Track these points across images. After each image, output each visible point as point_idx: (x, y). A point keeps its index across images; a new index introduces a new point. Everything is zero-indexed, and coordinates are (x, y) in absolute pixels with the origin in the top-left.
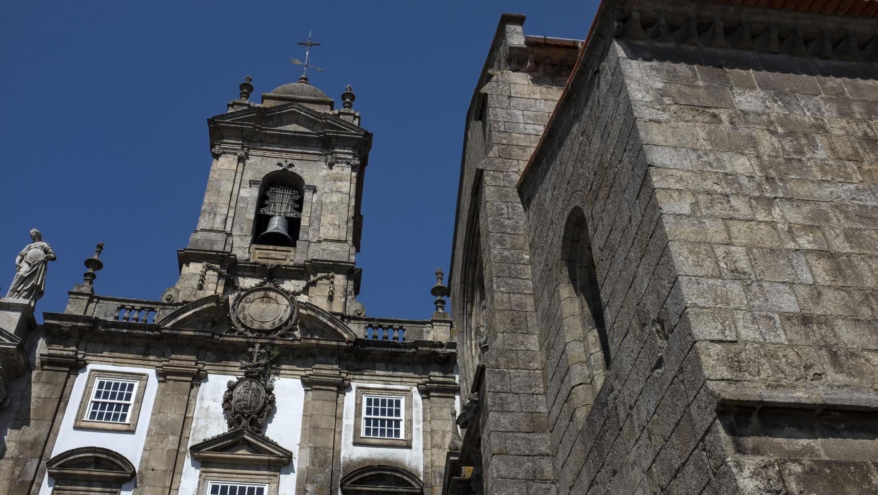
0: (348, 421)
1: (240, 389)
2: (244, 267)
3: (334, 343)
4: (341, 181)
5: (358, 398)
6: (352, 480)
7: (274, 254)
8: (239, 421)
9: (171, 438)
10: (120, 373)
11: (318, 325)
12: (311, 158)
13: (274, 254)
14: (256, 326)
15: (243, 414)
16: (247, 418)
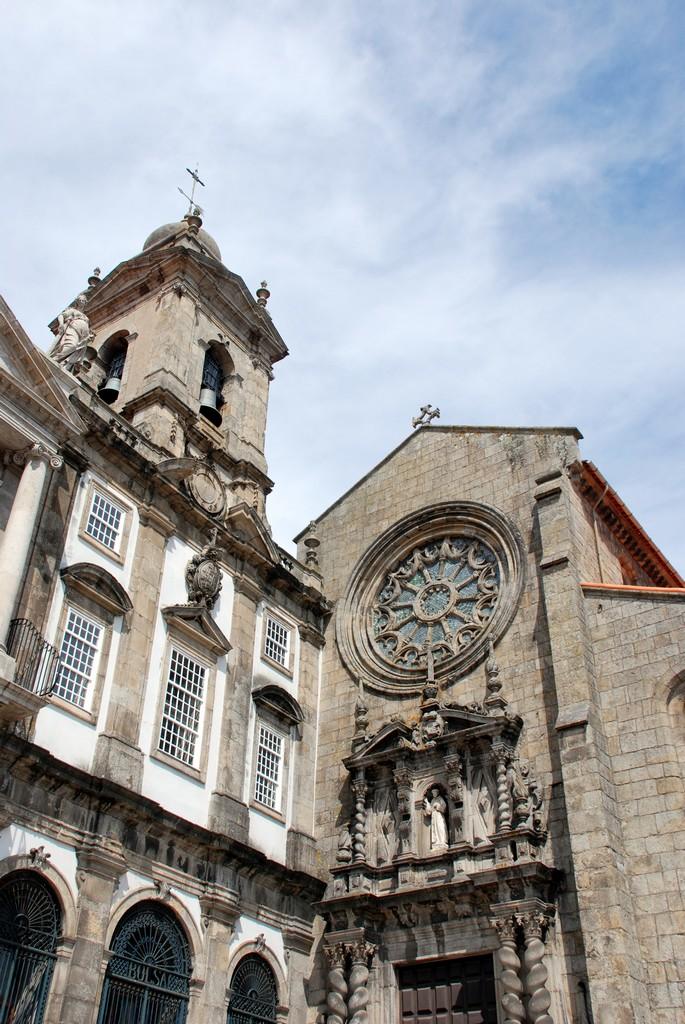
1: (205, 568)
2: (194, 433)
8: (198, 598)
10: (114, 496)
11: (251, 532)
12: (241, 346)
13: (213, 433)
16: (207, 598)
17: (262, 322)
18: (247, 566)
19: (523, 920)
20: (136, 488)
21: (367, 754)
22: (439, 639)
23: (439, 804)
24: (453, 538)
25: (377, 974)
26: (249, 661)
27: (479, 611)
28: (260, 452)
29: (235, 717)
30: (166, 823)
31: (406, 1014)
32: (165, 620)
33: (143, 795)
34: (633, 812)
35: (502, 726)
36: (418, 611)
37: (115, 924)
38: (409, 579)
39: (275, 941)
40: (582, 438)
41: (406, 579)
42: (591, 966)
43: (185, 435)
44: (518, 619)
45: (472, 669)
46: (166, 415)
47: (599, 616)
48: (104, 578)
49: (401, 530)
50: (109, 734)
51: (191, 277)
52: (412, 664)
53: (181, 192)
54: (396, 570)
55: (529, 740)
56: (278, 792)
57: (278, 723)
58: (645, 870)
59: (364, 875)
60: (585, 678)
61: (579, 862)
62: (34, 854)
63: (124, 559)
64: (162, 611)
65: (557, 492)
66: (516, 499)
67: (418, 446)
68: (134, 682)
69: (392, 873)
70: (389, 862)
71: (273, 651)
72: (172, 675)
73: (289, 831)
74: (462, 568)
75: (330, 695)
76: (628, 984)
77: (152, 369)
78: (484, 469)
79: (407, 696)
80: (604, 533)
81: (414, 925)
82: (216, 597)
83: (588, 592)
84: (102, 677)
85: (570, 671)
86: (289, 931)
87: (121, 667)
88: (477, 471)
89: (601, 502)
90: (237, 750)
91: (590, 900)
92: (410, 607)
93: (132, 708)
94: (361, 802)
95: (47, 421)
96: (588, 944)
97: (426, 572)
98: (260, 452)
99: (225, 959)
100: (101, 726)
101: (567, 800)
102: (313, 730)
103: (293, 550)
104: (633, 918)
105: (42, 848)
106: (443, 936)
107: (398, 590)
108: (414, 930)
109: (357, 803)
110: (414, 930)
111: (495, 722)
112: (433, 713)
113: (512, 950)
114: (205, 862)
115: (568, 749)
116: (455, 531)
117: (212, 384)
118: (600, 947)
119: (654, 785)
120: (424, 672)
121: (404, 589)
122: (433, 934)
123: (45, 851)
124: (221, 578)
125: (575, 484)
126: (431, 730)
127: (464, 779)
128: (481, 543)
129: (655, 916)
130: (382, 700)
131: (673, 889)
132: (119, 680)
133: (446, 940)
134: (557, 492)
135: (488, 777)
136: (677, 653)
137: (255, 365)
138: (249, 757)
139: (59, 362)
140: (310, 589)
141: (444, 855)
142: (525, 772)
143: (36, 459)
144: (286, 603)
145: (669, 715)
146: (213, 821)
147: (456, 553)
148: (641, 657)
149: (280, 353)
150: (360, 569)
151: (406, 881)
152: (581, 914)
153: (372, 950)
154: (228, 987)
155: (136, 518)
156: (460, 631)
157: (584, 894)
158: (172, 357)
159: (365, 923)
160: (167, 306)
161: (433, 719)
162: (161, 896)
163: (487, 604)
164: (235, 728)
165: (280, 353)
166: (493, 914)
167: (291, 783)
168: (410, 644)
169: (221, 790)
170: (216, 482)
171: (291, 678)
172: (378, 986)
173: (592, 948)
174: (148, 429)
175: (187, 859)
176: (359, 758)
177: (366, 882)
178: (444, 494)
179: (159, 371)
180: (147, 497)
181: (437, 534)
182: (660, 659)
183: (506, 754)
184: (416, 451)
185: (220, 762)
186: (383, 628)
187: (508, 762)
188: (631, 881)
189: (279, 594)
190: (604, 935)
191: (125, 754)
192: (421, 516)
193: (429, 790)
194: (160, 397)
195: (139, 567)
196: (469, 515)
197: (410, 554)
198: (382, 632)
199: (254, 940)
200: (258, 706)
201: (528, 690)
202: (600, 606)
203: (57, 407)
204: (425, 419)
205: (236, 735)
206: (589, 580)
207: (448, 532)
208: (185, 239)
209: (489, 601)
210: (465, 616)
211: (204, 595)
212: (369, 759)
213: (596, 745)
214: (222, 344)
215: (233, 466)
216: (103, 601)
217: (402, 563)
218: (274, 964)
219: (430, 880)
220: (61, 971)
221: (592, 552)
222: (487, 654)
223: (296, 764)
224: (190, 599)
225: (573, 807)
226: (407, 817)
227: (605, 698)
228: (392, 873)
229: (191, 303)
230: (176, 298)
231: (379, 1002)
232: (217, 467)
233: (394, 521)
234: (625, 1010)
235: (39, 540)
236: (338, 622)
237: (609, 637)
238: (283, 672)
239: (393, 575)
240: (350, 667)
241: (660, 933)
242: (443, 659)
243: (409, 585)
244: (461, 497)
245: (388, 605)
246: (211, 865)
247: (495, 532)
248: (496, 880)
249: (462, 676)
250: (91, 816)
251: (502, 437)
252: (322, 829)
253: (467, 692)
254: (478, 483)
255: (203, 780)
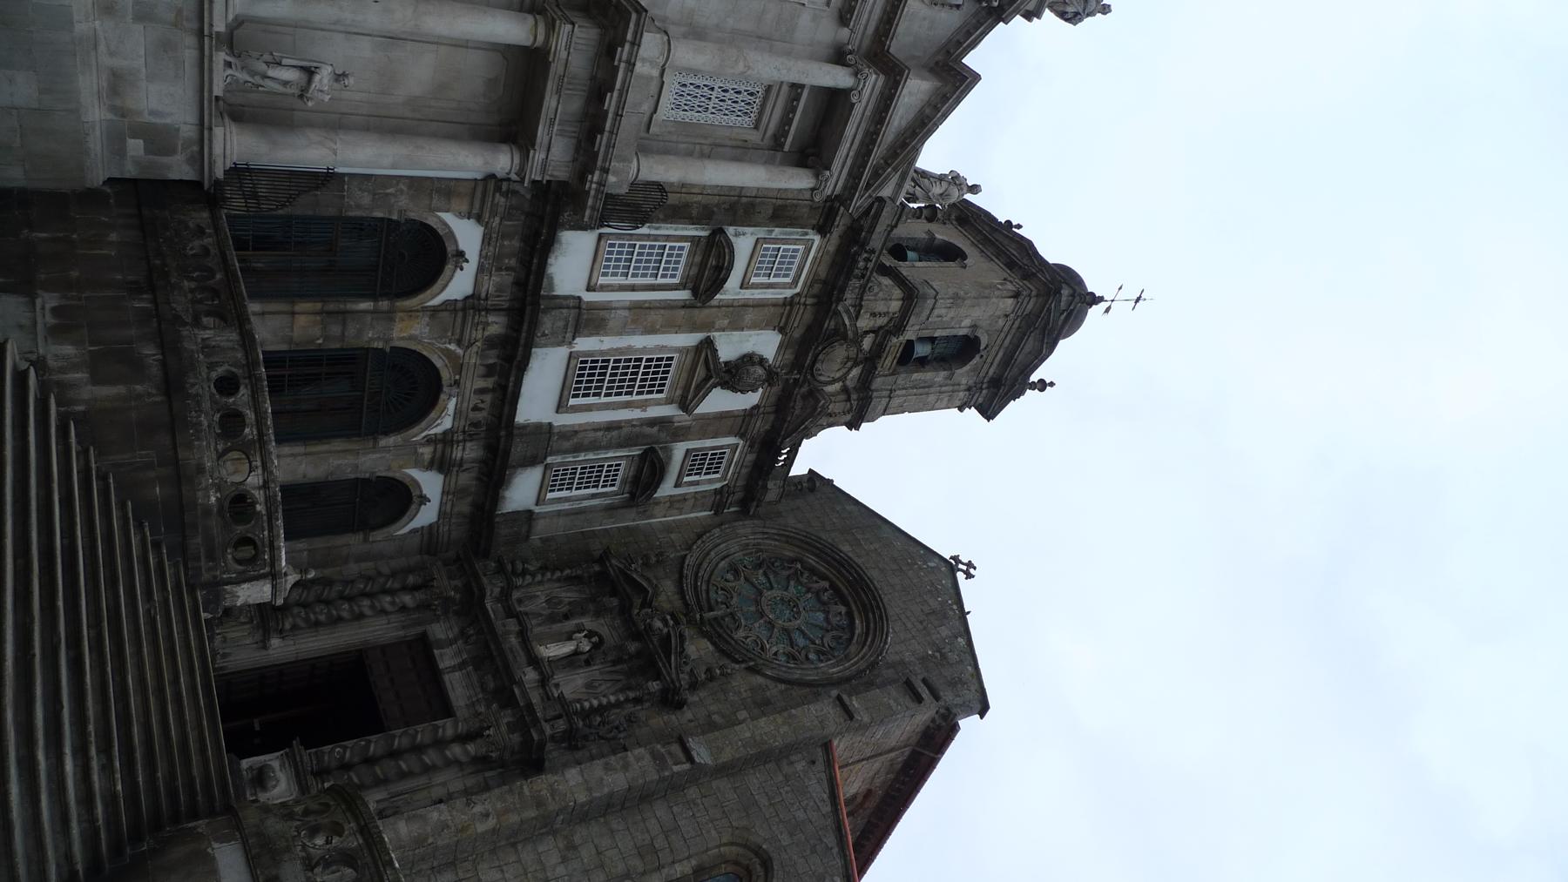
0: (709, 443)
1: (760, 371)
3: (783, 433)
4: (949, 400)
5: (728, 446)
6: (656, 461)
7: (890, 359)
9: (726, 322)
13: (890, 359)
14: (820, 357)
15: (734, 376)
17: (1013, 386)
18: (772, 417)
19: (488, 736)
20: (817, 288)
21: (619, 568)
22: (746, 619)
23: (586, 646)
24: (850, 615)
25: (417, 616)
26: (681, 438)
27: (781, 651)
28: (885, 410)
29: (625, 430)
30: (512, 379)
31: (384, 649)
32: (701, 342)
33: (533, 350)
34: (614, 826)
35: (671, 685)
36: (767, 594)
37: (413, 348)
38: (799, 582)
39: (426, 516)
40: (982, 718)
41: (798, 579)
42: (459, 803)
43: (881, 328)
44: (783, 687)
45: (722, 652)
46: (895, 306)
47: (804, 763)
48: (724, 272)
49: (842, 564)
50: (584, 306)
51: (1035, 305)
52: (716, 601)
53: (1120, 288)
54: (805, 569)
55: (666, 717)
56: (565, 494)
57: (629, 480)
58: (561, 845)
59: (502, 588)
60: (737, 756)
61: (556, 778)
62: (460, 255)
63: (747, 288)
64: (709, 337)
65: (919, 699)
66: (902, 662)
67: (930, 564)
68: (634, 321)
69: (510, 613)
70: (518, 609)
71: (696, 462)
72: (649, 360)
73: (530, 513)
74: (821, 628)
75: (668, 528)
76: (450, 838)
77: (934, 284)
78: (925, 628)
79: (683, 598)
80: (892, 765)
81: (466, 642)
82: (734, 390)
83: (827, 747)
84: (633, 288)
85: (740, 740)
86: (438, 527)
87: (647, 305)
88: (921, 622)
89: (923, 754)
90: (595, 441)
91: (521, 793)
92: (772, 588)
93: (611, 324)
94: (572, 573)
95: (855, 176)
96: (479, 797)
97: (809, 595)
98: (885, 410)
99: (401, 467)
100: (589, 297)
101: (613, 758)
102: (630, 520)
103: (799, 469)
104: (512, 840)
105: (467, 261)
106: (461, 670)
107: (786, 573)
108: (460, 642)
109: (571, 568)
110: (460, 642)
111: (674, 676)
112: (671, 623)
113: (459, 730)
114: (484, 428)
115: (663, 750)
116: (856, 614)
117: (937, 351)
118: (478, 809)
119: (647, 842)
120: (711, 609)
121: (788, 578)
122: (460, 660)
123: (464, 265)
124: (753, 391)
125: (933, 720)
126: (658, 624)
127: (614, 663)
128: (850, 640)
129: (519, 861)
130: (677, 576)
131: (549, 874)
132: (637, 307)
133: (457, 674)
134: (919, 699)
135: (619, 685)
136: (784, 843)
137: (969, 389)
138: (591, 456)
139: (913, 180)
140: (765, 487)
141: (536, 657)
142: (632, 719)
143: (817, 176)
144: (746, 467)
145: (718, 847)
146: (524, 427)
147: (834, 620)
148: (771, 810)
149: (989, 412)
150: (798, 534)
151: (505, 626)
152: (506, 788)
153: (434, 607)
154: (379, 474)
155: (788, 293)
156: (758, 637)
157: (525, 787)
158: (952, 301)
159: (458, 596)
160: (1000, 286)
161: (666, 623)
162: (445, 389)
163: (791, 657)
164: (615, 433)
165: (989, 412)
166: (488, 707)
167: (576, 505)
168: (735, 595)
169: (556, 431)
170: (844, 370)
171: (676, 486)
172: (403, 619)
173: (476, 801)
174: (876, 289)
175: (484, 409)
176: (614, 562)
177: (497, 590)
178: (890, 597)
179: (934, 289)
180: (810, 301)
181: (850, 598)
182: (774, 828)
183: (646, 697)
184: (925, 563)
185: (580, 425)
186: (744, 567)
187: (637, 701)
188: (548, 833)
189: (751, 457)
190: (490, 810)
191: (566, 327)
192: (863, 580)
193: (596, 634)
194: (911, 295)
195: (744, 306)
196: (875, 624)
197: (824, 577)
198: (741, 567)
199: (424, 492)
200: (640, 456)
201: (713, 708)
202: (813, 762)
203: (868, 186)
204: (960, 566)
205: (609, 436)
206: (840, 747)
207: (854, 608)
208: (1071, 292)
209: (794, 659)
210: (773, 640)
211: (734, 375)
212: (614, 570)
213: (672, 776)
214: (979, 351)
215: (865, 384)
216: (703, 276)
217: (813, 571)
218: (405, 519)
219: (512, 651)
220: (365, 305)
221: (868, 752)
222: (737, 662)
223: (595, 506)
224: (726, 363)
225: (607, 764)
226: (566, 617)
227: (722, 784)
228: (510, 613)
229: (1009, 310)
230: (1011, 294)
231: (389, 623)
232: (861, 366)
233: (850, 555)
234: (427, 838)
235: (744, 200)
236: (741, 523)
237: (785, 776)
238: (680, 476)
239: (799, 566)
240: (699, 542)
241: (505, 868)
242: (728, 627)
243: (792, 583)
244: (891, 612)
245: (768, 567)
246: (483, 435)
247: (864, 650)
248: (522, 704)
249: (714, 644)
250: (503, 303)
251: (960, 640)
252: (538, 543)
253: (698, 649)
254: (909, 625)
255: (560, 410)
